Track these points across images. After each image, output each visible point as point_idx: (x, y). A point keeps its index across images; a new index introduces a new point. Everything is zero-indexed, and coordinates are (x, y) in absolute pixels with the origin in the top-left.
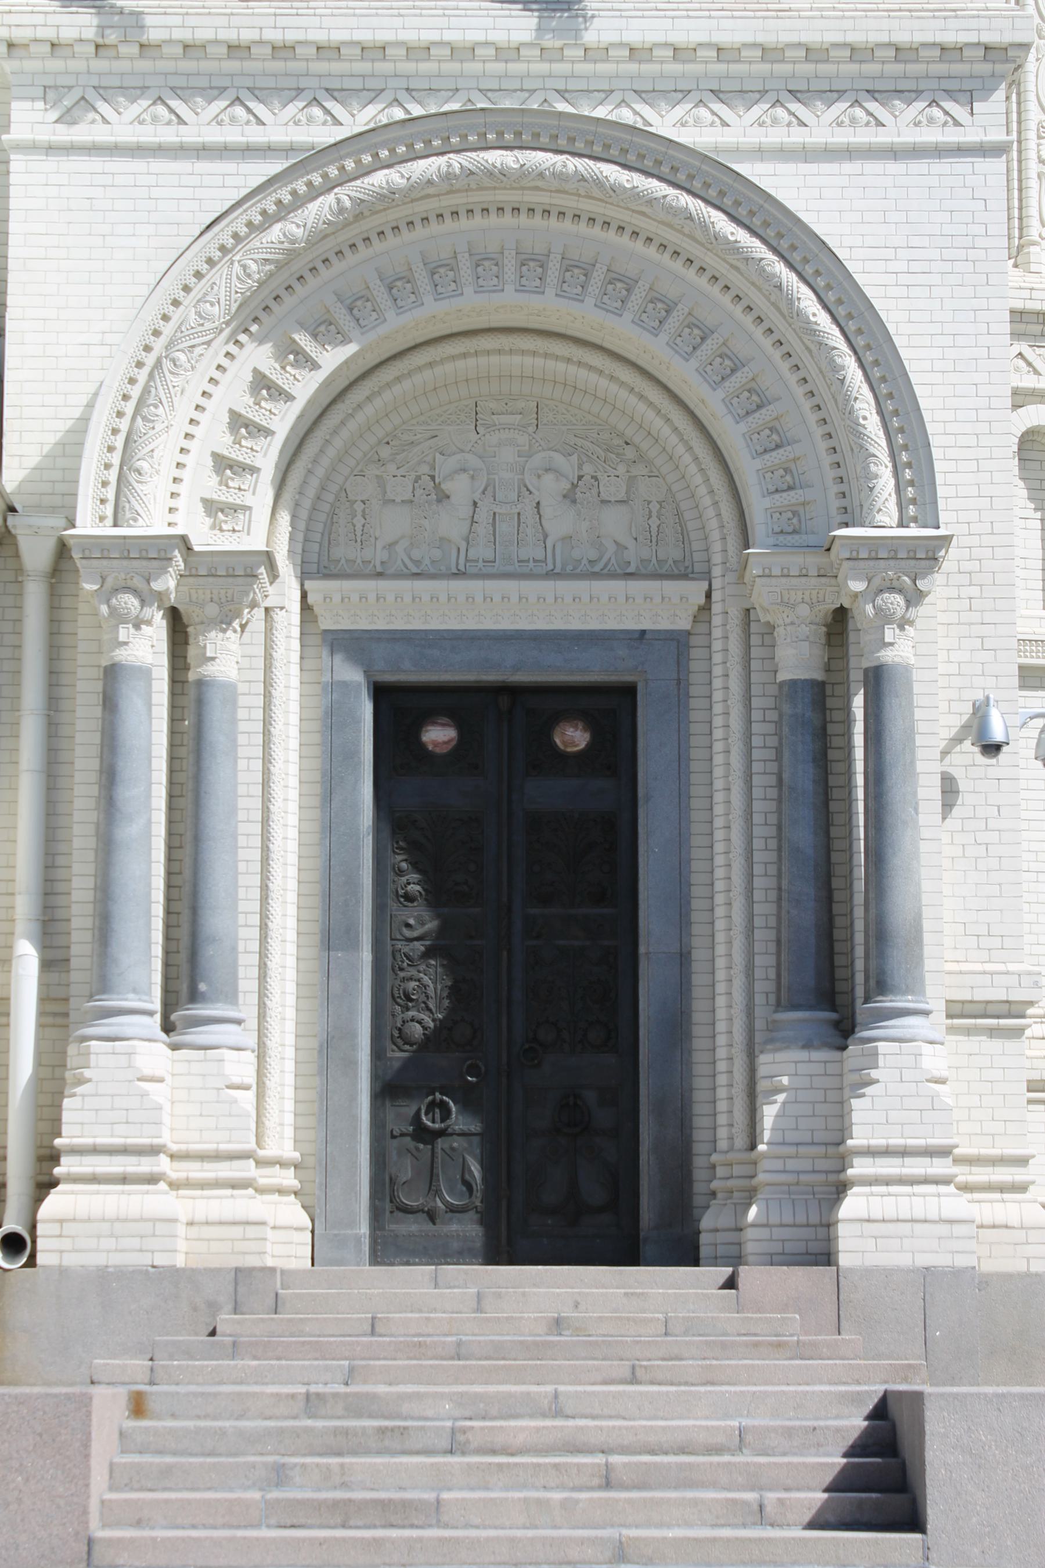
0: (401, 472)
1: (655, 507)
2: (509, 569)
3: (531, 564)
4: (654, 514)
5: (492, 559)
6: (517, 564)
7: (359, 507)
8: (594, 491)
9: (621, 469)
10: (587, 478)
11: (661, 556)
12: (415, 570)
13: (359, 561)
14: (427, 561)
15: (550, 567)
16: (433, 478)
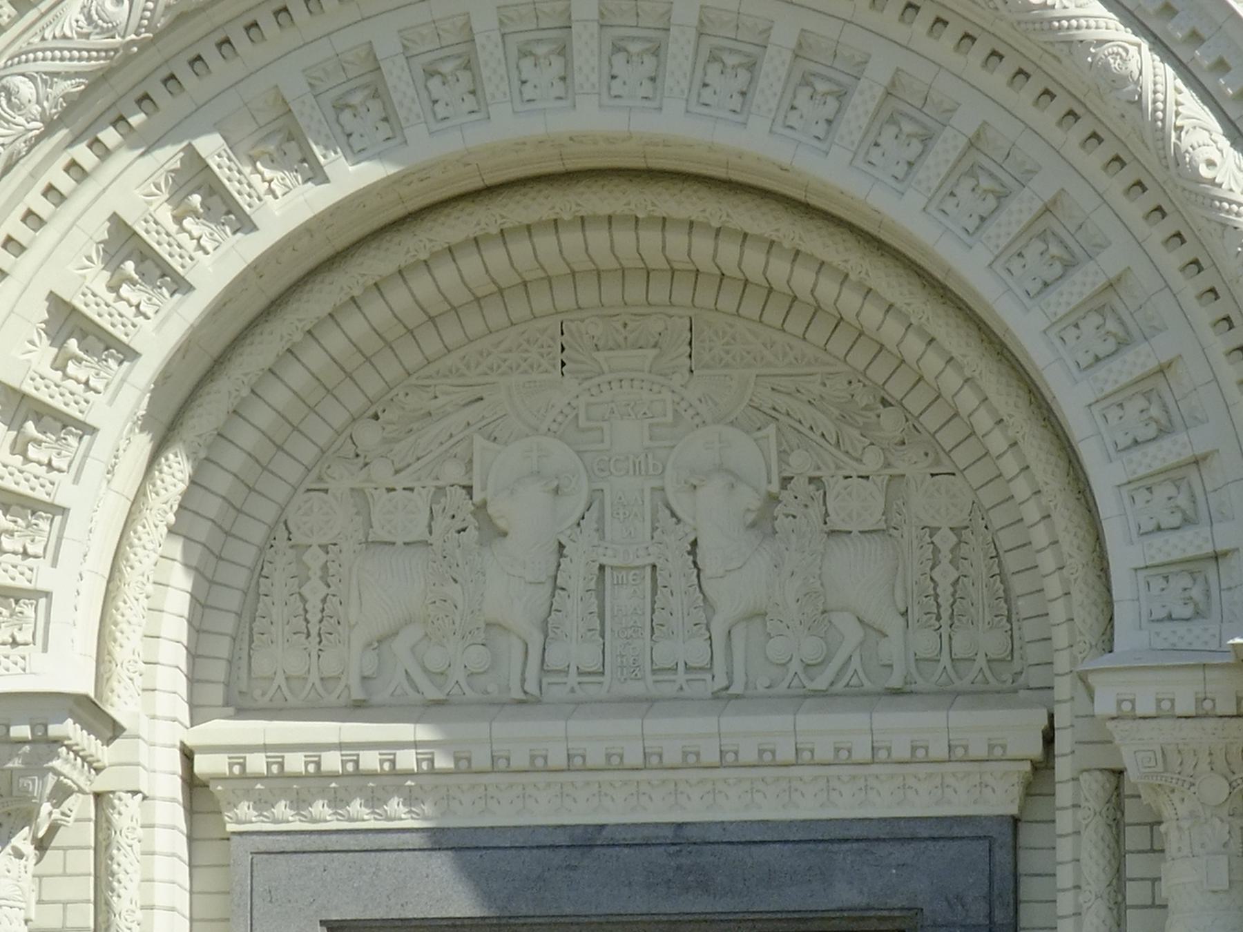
0: (404, 480)
1: (946, 541)
2: (636, 688)
3: (681, 676)
4: (945, 556)
5: (598, 668)
6: (650, 678)
7: (314, 559)
8: (815, 512)
9: (872, 461)
10: (799, 484)
11: (959, 651)
12: (433, 694)
13: (314, 677)
14: (458, 674)
15: (721, 682)
16: (469, 489)
